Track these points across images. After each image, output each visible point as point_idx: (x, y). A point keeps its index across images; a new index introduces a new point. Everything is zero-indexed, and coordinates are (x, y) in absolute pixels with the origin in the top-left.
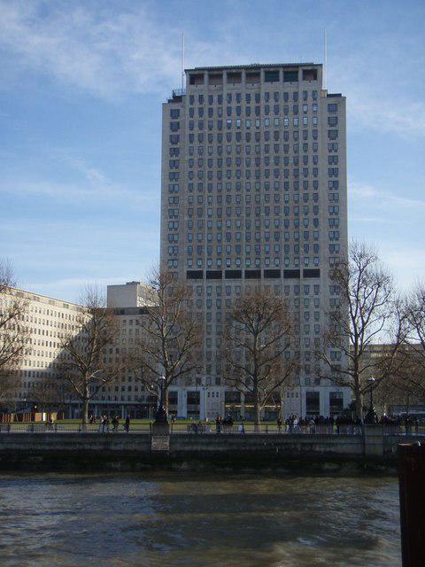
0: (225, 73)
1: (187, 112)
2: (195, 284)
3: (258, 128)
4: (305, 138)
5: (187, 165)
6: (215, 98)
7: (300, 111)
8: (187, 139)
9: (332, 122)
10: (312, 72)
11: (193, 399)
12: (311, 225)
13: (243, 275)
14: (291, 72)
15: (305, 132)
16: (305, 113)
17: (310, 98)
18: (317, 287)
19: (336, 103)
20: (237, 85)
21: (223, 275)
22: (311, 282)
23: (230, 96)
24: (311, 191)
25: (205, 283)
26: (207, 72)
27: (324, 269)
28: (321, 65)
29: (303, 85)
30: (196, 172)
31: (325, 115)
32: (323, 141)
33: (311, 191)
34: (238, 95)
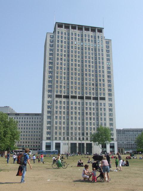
0: (70, 25)
2: (59, 100)
3: (82, 46)
4: (99, 51)
7: (97, 42)
9: (108, 47)
10: (100, 30)
11: (58, 146)
13: (77, 97)
14: (93, 29)
15: (99, 49)
16: (99, 43)
17: (100, 38)
18: (105, 104)
19: (108, 42)
20: (75, 30)
21: (70, 97)
22: (102, 102)
24: (101, 69)
26: (64, 24)
27: (107, 97)
28: (103, 28)
29: (98, 34)
30: (60, 58)
31: (105, 45)
32: (105, 53)
33: (101, 69)
34: (75, 34)
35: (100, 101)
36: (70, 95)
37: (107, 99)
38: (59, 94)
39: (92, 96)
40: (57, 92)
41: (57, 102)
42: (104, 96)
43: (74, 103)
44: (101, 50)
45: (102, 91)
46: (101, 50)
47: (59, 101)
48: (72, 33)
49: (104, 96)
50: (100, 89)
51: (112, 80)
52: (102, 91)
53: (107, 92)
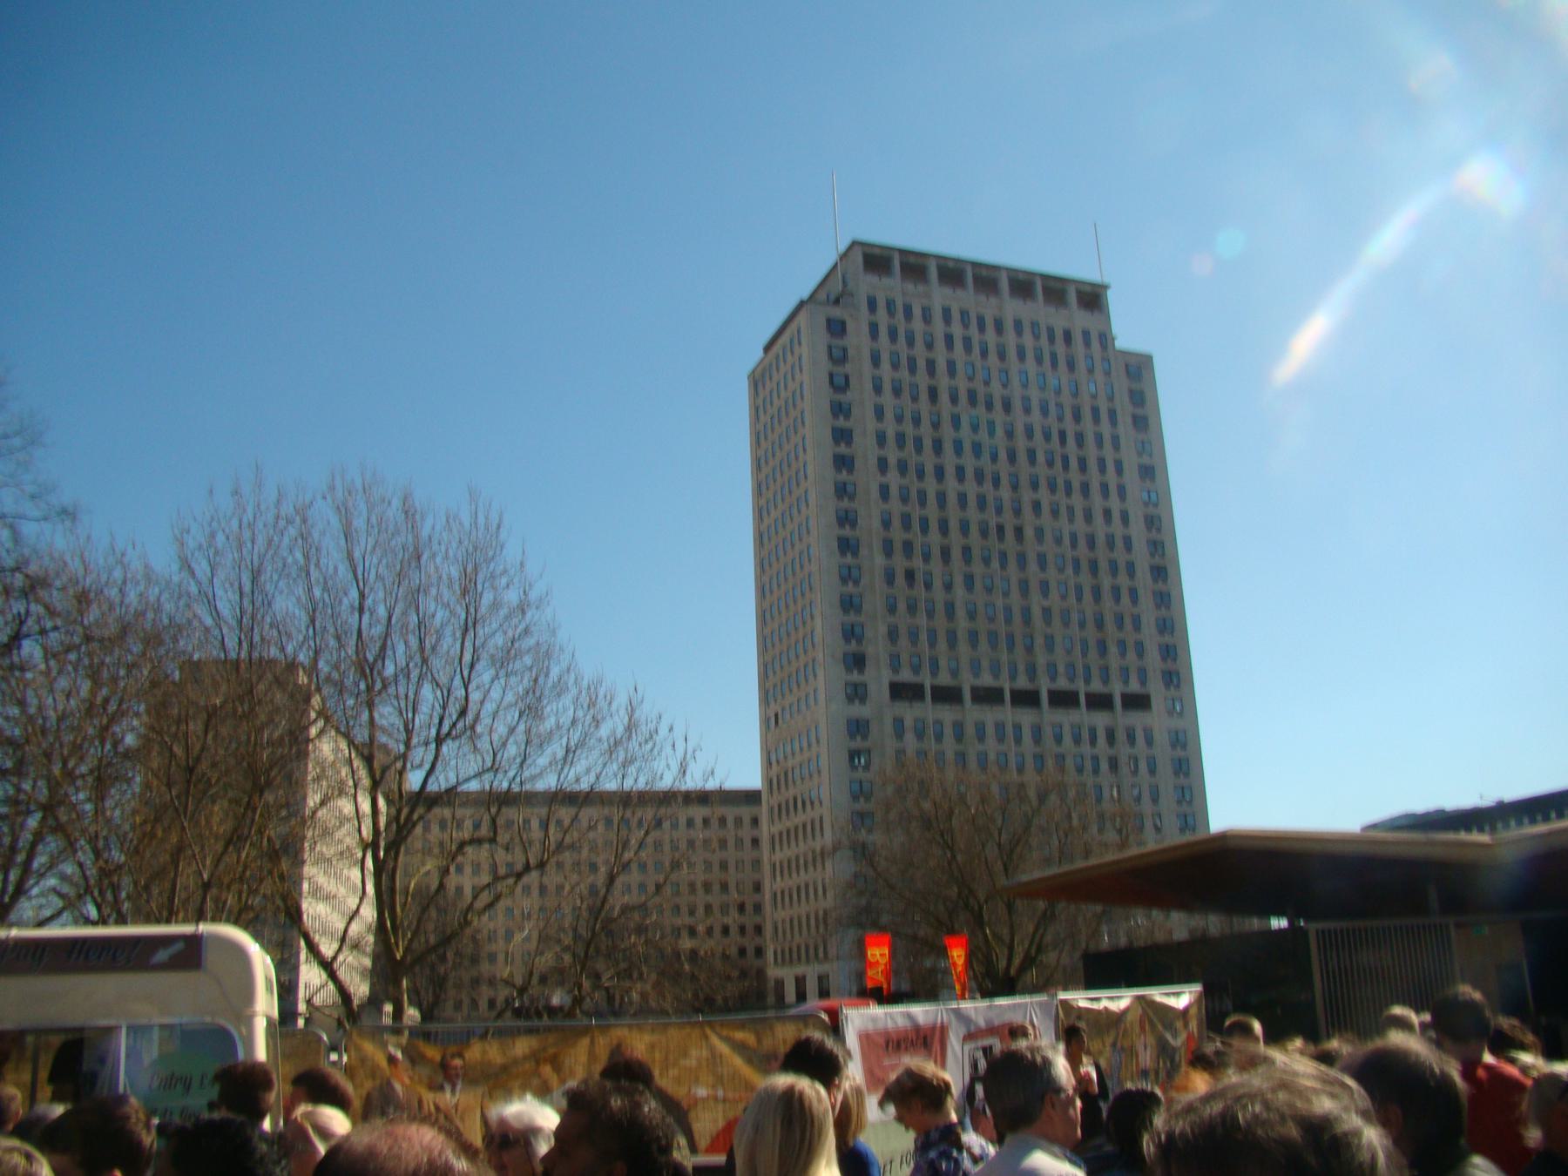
1: (865, 329)
2: (910, 712)
5: (871, 441)
6: (917, 312)
8: (869, 386)
10: (1093, 298)
12: (1126, 599)
14: (1055, 289)
15: (1095, 411)
20: (960, 293)
22: (1136, 719)
23: (947, 313)
25: (928, 711)
27: (1156, 690)
29: (1080, 319)
31: (1121, 385)
33: (1117, 528)
34: (964, 314)
35: (1124, 719)
36: (967, 682)
37: (1157, 702)
38: (906, 676)
39: (1081, 688)
40: (976, 671)
41: (899, 723)
42: (1143, 683)
43: (990, 731)
44: (1104, 416)
45: (1131, 656)
46: (1104, 416)
47: (908, 723)
48: (947, 313)
49: (1143, 683)
50: (1122, 644)
51: (1174, 593)
52: (1131, 656)
53: (1153, 659)
